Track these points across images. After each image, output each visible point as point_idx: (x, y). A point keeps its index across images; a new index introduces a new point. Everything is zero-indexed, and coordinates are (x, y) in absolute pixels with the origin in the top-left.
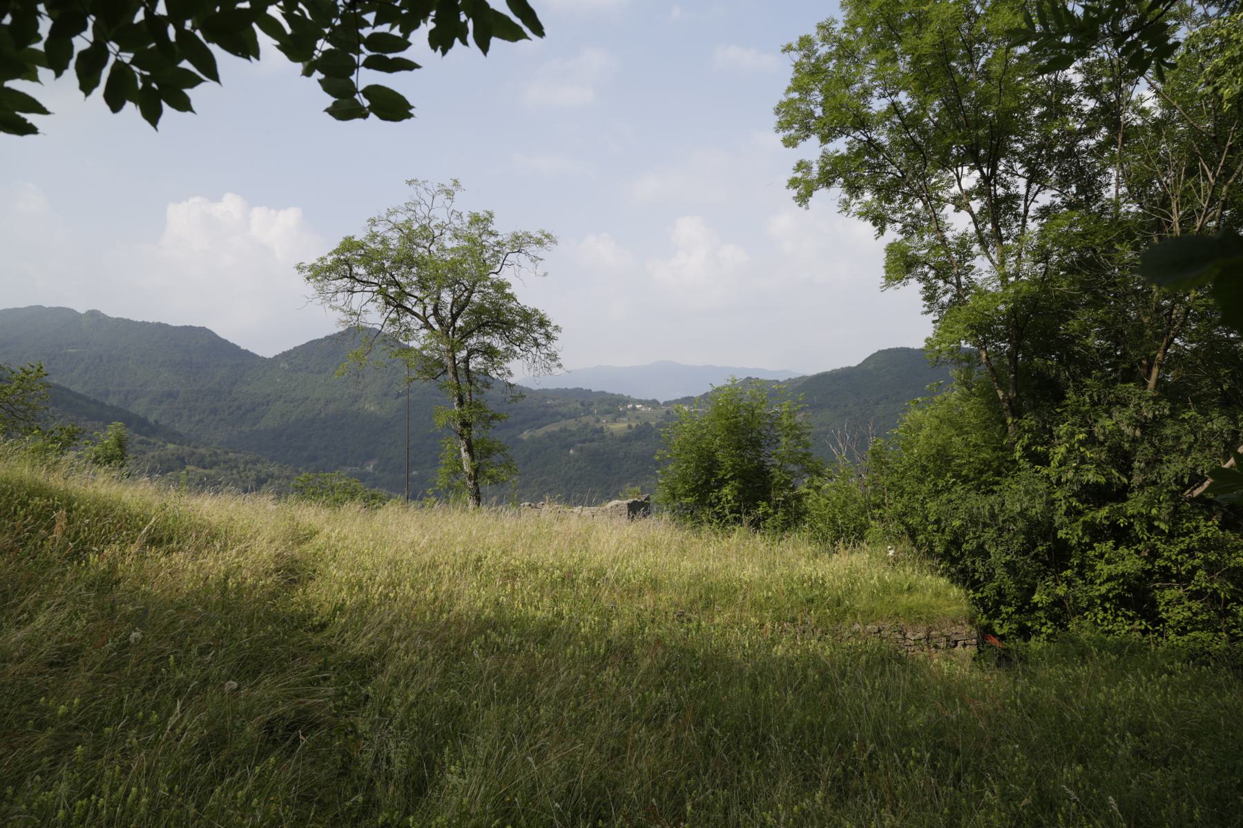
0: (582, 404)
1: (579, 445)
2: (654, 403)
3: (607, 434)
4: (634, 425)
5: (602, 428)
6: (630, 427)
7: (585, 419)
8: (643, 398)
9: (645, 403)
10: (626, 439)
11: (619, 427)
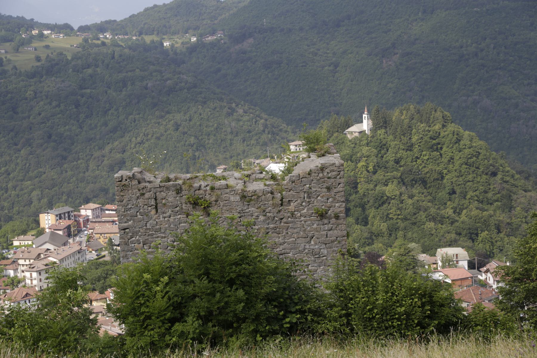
2: (66, 29)
3: (9, 68)
4: (43, 56)
6: (38, 59)
8: (52, 22)
9: (55, 28)
10: (34, 74)
11: (25, 59)
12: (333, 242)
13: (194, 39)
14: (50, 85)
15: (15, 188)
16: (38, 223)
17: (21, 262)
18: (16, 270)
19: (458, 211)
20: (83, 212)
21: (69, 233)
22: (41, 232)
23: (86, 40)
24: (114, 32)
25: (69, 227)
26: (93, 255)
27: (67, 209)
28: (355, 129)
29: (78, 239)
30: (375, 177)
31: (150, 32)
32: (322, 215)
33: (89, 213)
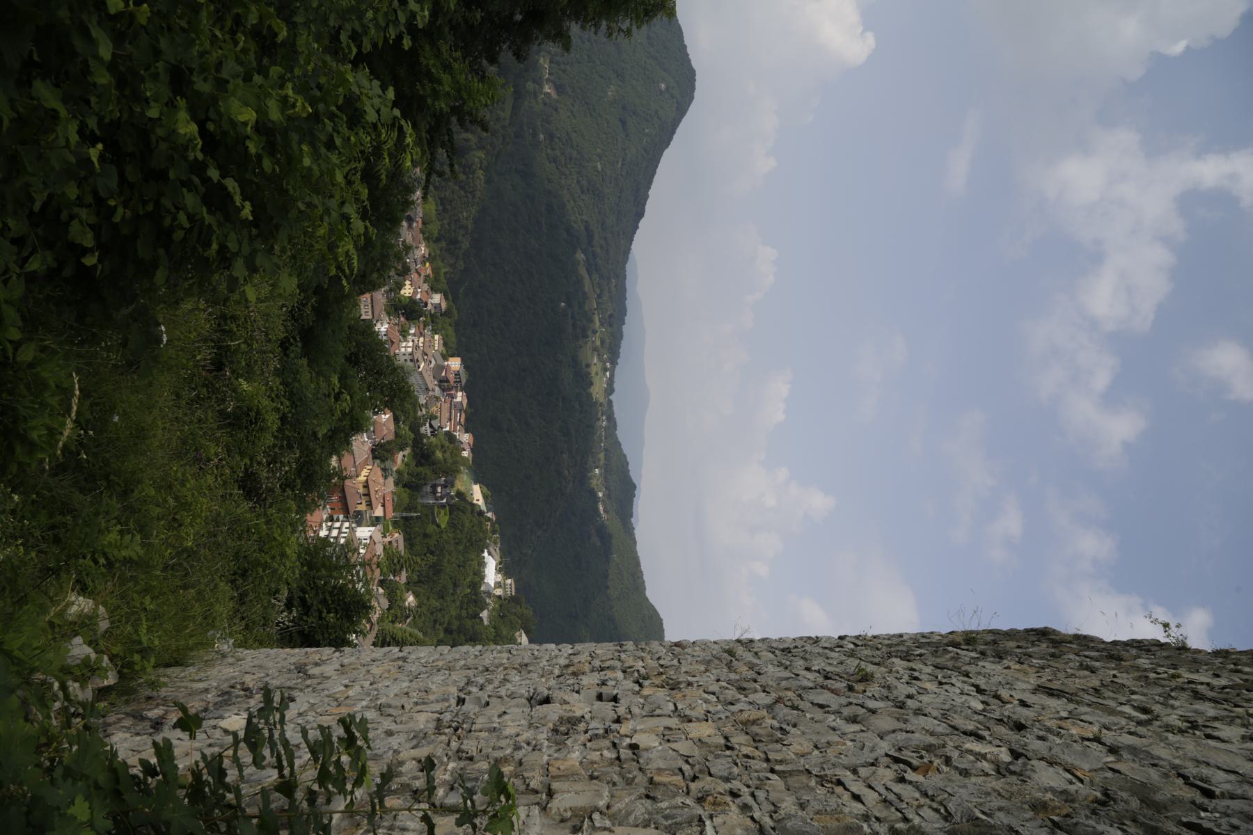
0: (611, 316)
2: (610, 390)
5: (587, 337)
7: (596, 319)
8: (616, 380)
9: (611, 382)
10: (575, 362)
13: (600, 494)
16: (453, 356)
17: (422, 339)
18: (414, 335)
20: (460, 394)
21: (443, 383)
22: (445, 358)
23: (601, 405)
24: (605, 428)
25: (448, 381)
26: (422, 400)
29: (437, 388)
33: (459, 399)
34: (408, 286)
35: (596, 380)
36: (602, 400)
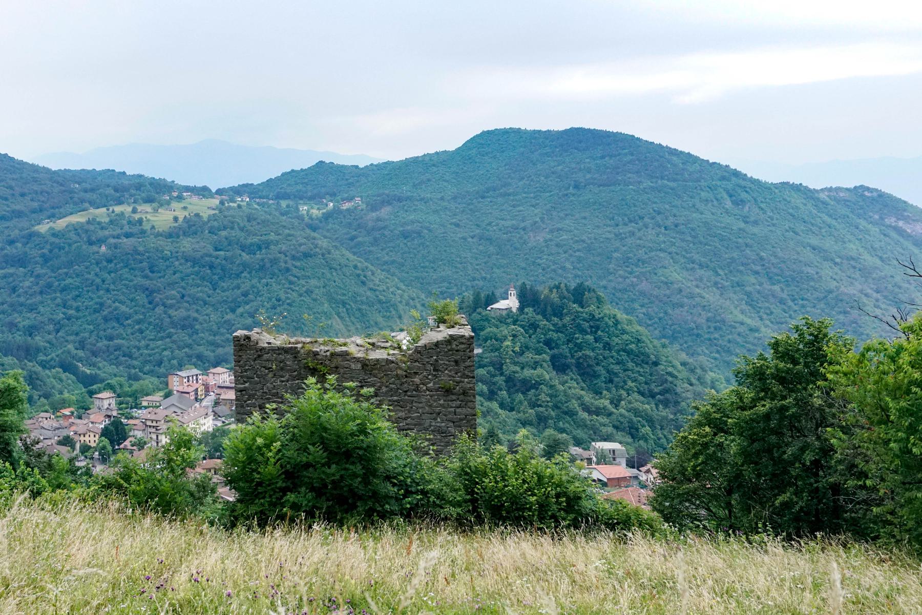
0: (116, 190)
1: (112, 241)
2: (203, 192)
3: (146, 226)
5: (140, 221)
6: (176, 219)
10: (171, 235)
11: (162, 218)
12: (461, 420)
14: (187, 245)
15: (147, 346)
19: (616, 403)
27: (195, 371)
28: (502, 304)
30: (522, 359)
31: (286, 196)
32: (448, 391)
34: (87, 438)
35: (193, 209)
36: (215, 202)
